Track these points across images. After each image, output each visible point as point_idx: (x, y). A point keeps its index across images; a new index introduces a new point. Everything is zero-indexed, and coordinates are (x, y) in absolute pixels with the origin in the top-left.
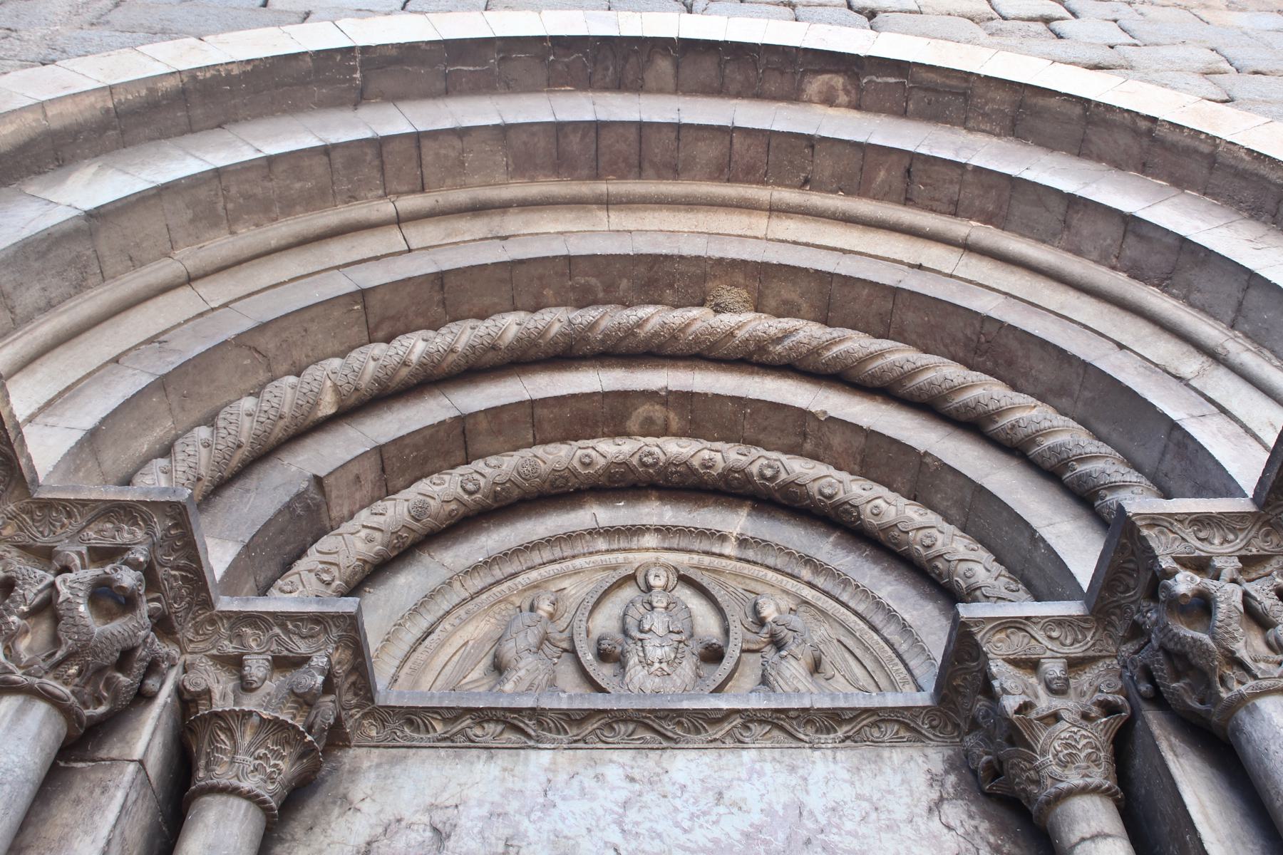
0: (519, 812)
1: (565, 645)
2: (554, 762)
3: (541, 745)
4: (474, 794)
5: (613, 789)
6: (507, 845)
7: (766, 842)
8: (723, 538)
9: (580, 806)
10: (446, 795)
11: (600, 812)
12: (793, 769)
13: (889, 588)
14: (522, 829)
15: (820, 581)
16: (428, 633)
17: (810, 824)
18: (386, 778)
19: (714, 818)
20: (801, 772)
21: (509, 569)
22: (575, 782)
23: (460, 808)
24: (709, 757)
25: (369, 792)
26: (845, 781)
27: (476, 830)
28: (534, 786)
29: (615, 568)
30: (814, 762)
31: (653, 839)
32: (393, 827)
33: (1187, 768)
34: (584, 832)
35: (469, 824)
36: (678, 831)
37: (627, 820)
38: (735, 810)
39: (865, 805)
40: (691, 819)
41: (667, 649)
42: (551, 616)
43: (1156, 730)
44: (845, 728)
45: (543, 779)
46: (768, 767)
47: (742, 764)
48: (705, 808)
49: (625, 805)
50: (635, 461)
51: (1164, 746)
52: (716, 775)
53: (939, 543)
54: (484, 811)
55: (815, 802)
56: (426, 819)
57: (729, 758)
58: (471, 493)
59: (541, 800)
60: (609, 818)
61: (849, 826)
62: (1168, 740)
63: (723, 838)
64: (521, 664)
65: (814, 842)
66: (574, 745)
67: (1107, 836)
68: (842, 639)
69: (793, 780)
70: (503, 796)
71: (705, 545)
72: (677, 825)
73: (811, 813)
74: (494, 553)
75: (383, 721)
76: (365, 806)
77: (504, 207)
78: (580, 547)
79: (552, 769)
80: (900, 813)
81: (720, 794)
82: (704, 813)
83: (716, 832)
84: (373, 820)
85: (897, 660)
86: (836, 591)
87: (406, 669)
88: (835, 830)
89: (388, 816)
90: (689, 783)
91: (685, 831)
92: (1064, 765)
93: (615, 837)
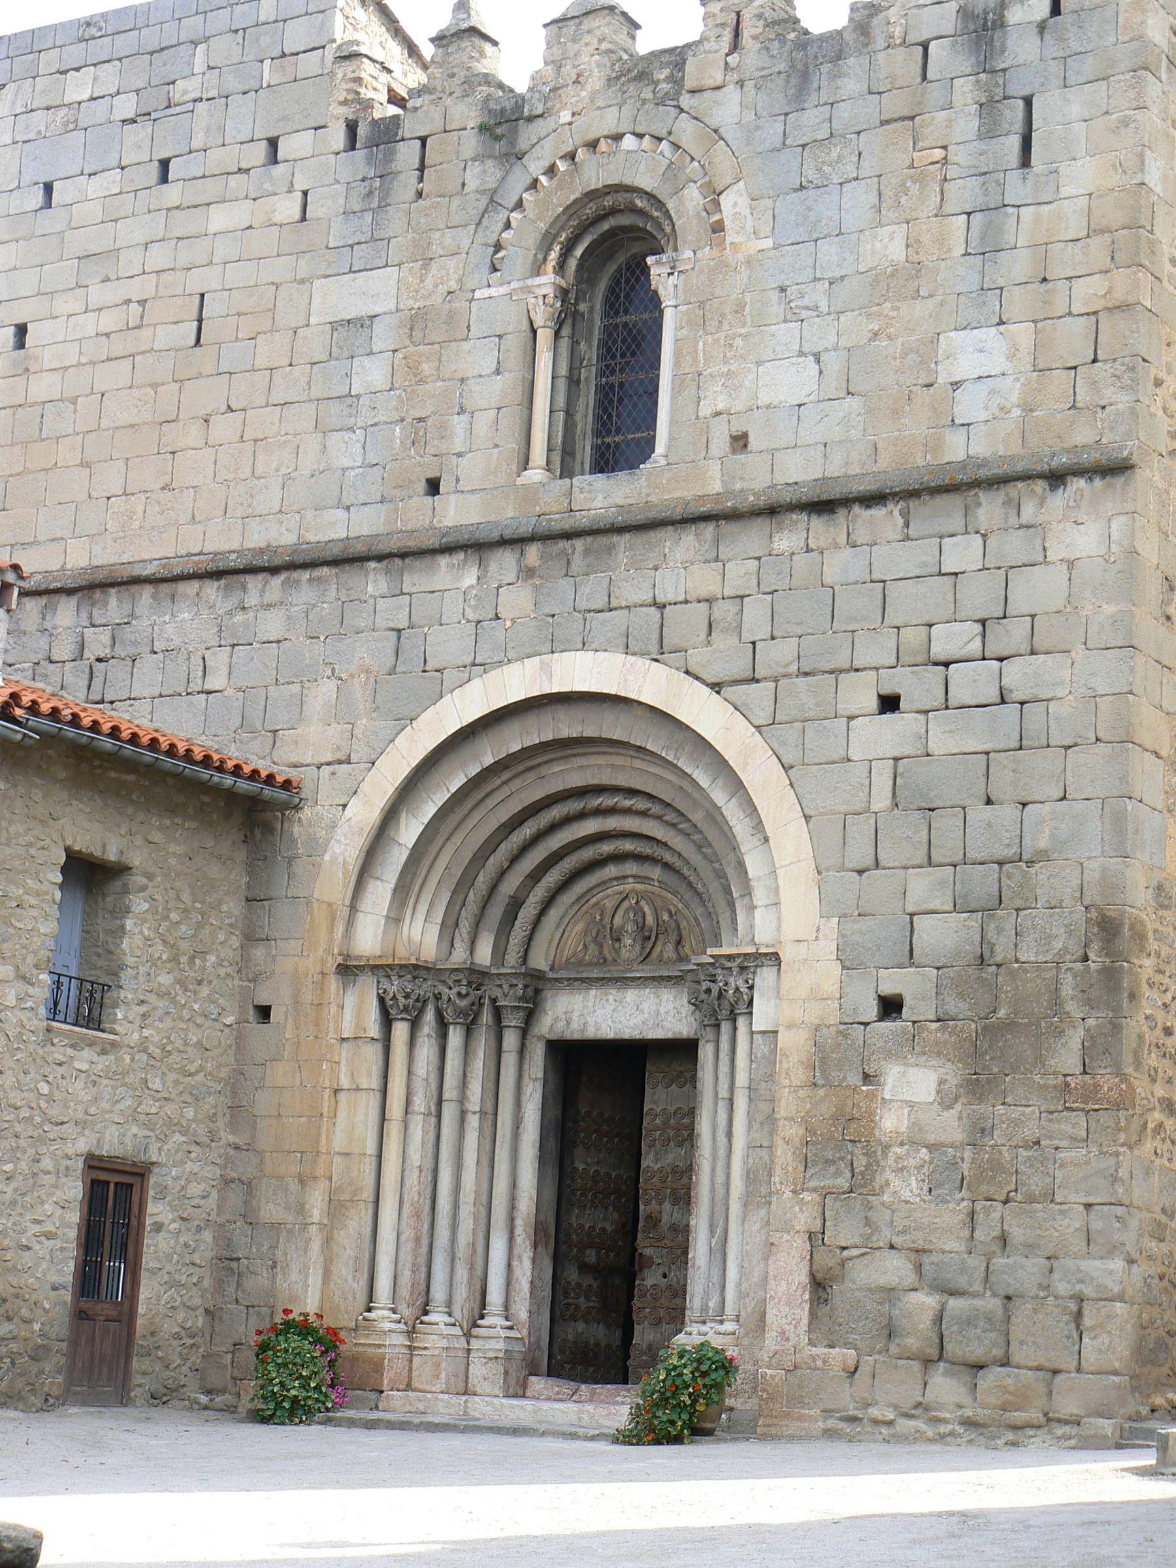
4: (576, 1007)
9: (602, 1011)
28: (590, 1004)
29: (621, 893)
42: (601, 920)
77: (539, 765)
79: (595, 997)
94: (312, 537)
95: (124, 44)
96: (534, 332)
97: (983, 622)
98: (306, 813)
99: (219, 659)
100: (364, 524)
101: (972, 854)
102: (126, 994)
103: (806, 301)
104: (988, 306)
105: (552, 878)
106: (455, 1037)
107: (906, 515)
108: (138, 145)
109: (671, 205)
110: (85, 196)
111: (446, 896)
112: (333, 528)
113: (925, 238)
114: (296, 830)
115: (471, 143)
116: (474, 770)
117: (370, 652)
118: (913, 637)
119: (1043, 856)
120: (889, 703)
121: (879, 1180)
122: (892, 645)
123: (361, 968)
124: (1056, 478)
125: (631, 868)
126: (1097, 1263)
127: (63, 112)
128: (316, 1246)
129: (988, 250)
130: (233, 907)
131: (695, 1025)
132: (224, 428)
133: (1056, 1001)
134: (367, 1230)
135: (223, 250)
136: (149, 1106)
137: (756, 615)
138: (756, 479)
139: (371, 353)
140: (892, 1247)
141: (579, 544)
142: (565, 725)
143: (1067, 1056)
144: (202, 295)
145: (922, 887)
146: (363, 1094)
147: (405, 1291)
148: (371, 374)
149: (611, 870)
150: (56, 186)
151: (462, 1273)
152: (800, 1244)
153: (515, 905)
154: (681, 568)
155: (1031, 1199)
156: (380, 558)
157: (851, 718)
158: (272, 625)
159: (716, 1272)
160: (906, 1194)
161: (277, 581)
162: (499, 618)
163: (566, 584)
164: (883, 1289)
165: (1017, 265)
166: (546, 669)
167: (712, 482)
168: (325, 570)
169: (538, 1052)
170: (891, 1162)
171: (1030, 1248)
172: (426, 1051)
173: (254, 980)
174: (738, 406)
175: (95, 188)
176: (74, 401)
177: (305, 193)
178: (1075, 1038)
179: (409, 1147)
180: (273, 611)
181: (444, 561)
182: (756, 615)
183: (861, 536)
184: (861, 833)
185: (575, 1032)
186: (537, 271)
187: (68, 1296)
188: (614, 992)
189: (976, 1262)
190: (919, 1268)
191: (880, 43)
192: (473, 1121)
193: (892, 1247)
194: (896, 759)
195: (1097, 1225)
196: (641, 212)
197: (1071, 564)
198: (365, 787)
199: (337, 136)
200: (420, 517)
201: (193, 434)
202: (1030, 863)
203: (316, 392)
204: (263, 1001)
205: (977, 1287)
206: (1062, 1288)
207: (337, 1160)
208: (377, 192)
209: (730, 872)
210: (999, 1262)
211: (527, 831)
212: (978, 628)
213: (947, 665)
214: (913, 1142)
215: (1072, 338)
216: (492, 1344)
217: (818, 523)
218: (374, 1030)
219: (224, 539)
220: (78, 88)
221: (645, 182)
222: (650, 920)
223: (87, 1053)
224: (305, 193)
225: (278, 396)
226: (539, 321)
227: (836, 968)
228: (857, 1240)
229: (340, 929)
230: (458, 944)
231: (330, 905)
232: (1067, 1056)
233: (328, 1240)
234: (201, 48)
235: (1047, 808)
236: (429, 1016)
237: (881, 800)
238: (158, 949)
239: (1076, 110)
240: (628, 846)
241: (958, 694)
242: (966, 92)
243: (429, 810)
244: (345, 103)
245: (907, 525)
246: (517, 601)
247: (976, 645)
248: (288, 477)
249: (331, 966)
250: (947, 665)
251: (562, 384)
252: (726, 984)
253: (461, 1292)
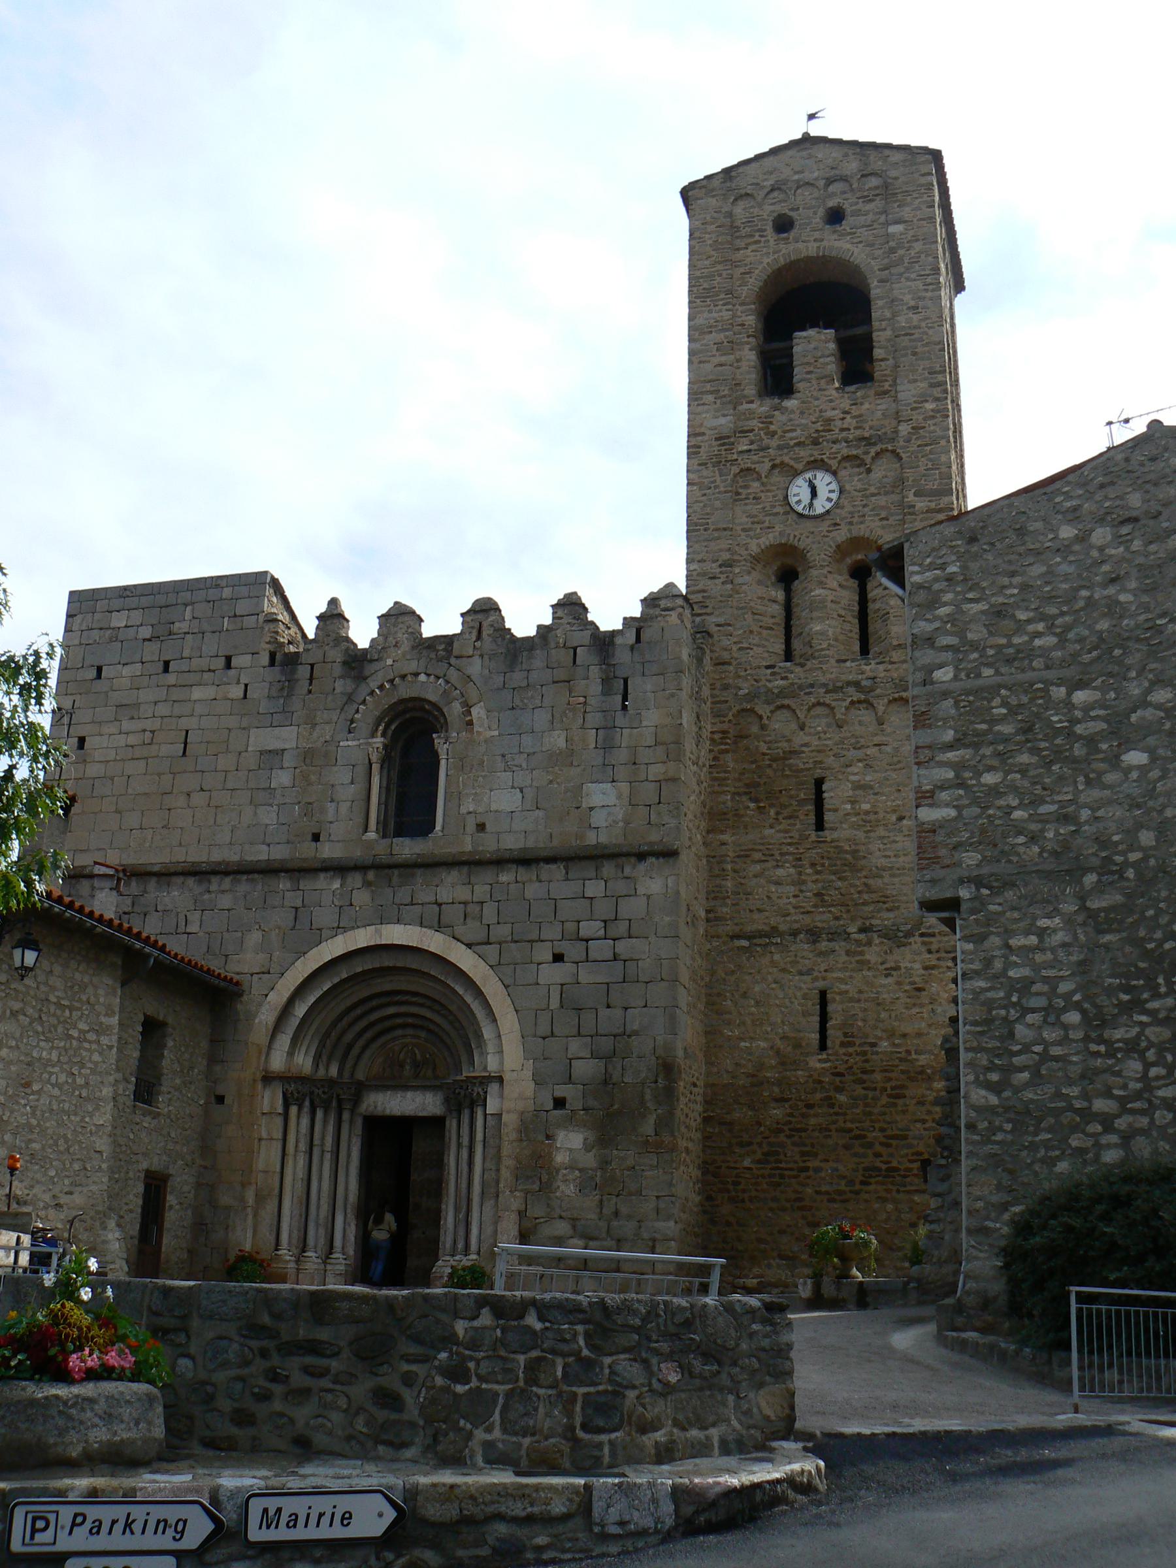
94: (248, 858)
95: (145, 601)
96: (371, 765)
97: (605, 922)
98: (245, 998)
99: (195, 917)
100: (279, 853)
101: (601, 1031)
102: (164, 1089)
103: (515, 762)
104: (607, 772)
106: (320, 1114)
107: (566, 868)
108: (152, 651)
109: (445, 710)
110: (122, 675)
112: (261, 854)
113: (576, 738)
114: (239, 1007)
115: (338, 669)
116: (336, 980)
117: (280, 918)
118: (570, 927)
119: (636, 1033)
120: (558, 958)
121: (555, 1185)
122: (559, 929)
123: (274, 1078)
124: (641, 856)
125: (410, 1031)
126: (663, 1224)
127: (109, 632)
128: (250, 1217)
129: (607, 747)
130: (204, 1044)
132: (198, 799)
133: (643, 1103)
134: (276, 1210)
135: (199, 709)
136: (170, 1146)
137: (489, 911)
138: (489, 845)
139: (282, 768)
140: (561, 1217)
141: (396, 872)
142: (387, 961)
143: (648, 1127)
144: (187, 732)
145: (576, 1047)
146: (274, 1142)
147: (294, 1241)
148: (282, 778)
149: (399, 1032)
150: (104, 668)
151: (322, 1231)
152: (514, 1217)
153: (350, 1047)
154: (450, 888)
155: (630, 1194)
156: (287, 871)
157: (539, 964)
158: (225, 901)
159: (461, 1232)
160: (568, 1192)
161: (228, 880)
162: (351, 905)
163: (389, 892)
164: (555, 1237)
165: (622, 755)
166: (378, 932)
167: (467, 845)
168: (256, 876)
169: (359, 1122)
170: (560, 1177)
171: (629, 1217)
172: (305, 1121)
173: (215, 1082)
174: (480, 810)
175: (126, 671)
176: (112, 779)
177: (246, 685)
178: (652, 1119)
179: (296, 1168)
180: (226, 895)
181: (322, 875)
182: (489, 911)
183: (544, 877)
184: (544, 1019)
185: (379, 1111)
186: (373, 736)
187: (136, 1242)
189: (603, 1224)
190: (574, 1227)
191: (553, 645)
192: (328, 1156)
193: (561, 1217)
194: (562, 985)
195: (662, 1205)
196: (428, 712)
197: (648, 897)
198: (278, 986)
199: (265, 660)
200: (307, 850)
201: (182, 801)
202: (629, 1036)
203: (252, 785)
204: (220, 1092)
205: (604, 1235)
206: (646, 1235)
207: (260, 1176)
208: (287, 687)
209: (471, 1035)
210: (615, 1223)
211: (359, 1011)
212: (603, 924)
213: (587, 941)
214: (571, 1167)
215: (648, 792)
216: (338, 1267)
217: (522, 870)
218: (280, 1110)
219: (197, 855)
220: (119, 620)
221: (432, 698)
222: (419, 1057)
223: (148, 1119)
224: (246, 685)
225: (230, 785)
226: (374, 758)
227: (532, 1085)
228: (543, 1214)
229: (263, 1058)
230: (321, 1066)
231: (258, 1045)
232: (648, 1127)
233: (255, 1215)
234: (189, 608)
235: (636, 1011)
236: (307, 1103)
237: (555, 1003)
238: (176, 1067)
239: (649, 687)
241: (593, 955)
242: (595, 672)
243: (312, 999)
244: (269, 643)
245: (567, 873)
246: (362, 897)
247: (602, 932)
248: (234, 827)
249: (259, 1076)
250: (587, 941)
251: (384, 790)
253: (322, 1241)
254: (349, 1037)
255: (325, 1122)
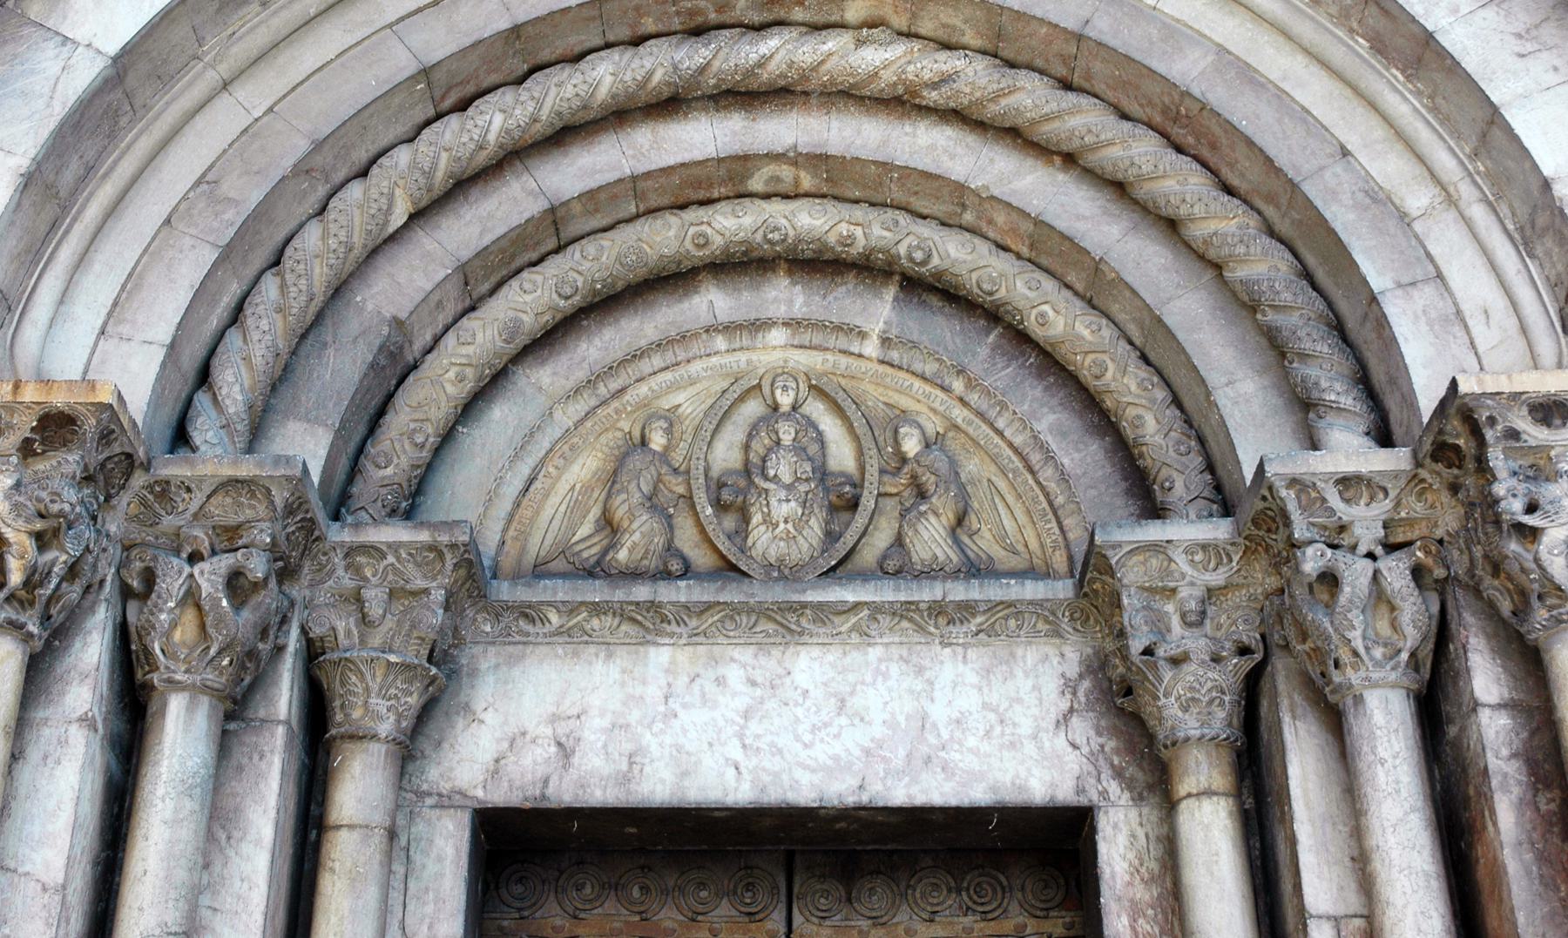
0: (640, 722)
1: (681, 490)
2: (673, 662)
3: (659, 640)
4: (595, 701)
5: (734, 694)
6: (631, 764)
7: (885, 759)
8: (863, 335)
9: (700, 716)
10: (567, 703)
11: (721, 723)
12: (920, 671)
13: (1052, 418)
14: (644, 743)
15: (974, 398)
16: (531, 481)
17: (932, 740)
18: (506, 682)
19: (834, 730)
20: (928, 674)
21: (614, 385)
22: (696, 687)
23: (583, 718)
24: (833, 655)
25: (491, 700)
26: (973, 686)
27: (600, 744)
28: (654, 692)
30: (942, 662)
31: (773, 755)
32: (519, 742)
33: (1302, 733)
34: (706, 746)
35: (592, 737)
36: (799, 746)
37: (748, 733)
38: (857, 721)
39: (992, 717)
40: (812, 732)
41: (793, 504)
43: (1282, 685)
44: (979, 619)
45: (663, 682)
46: (894, 669)
47: (867, 664)
48: (826, 719)
49: (747, 715)
50: (759, 237)
51: (1284, 704)
52: (839, 678)
53: (1109, 375)
54: (605, 722)
55: (939, 712)
56: (549, 731)
57: (855, 657)
58: (567, 298)
59: (662, 708)
60: (730, 730)
61: (972, 742)
62: (1291, 697)
63: (843, 755)
64: (635, 526)
65: (935, 760)
66: (695, 639)
67: (1215, 794)
68: (994, 478)
69: (919, 685)
70: (624, 704)
71: (842, 342)
72: (797, 738)
73: (934, 725)
74: (597, 368)
75: (497, 615)
76: (489, 717)
78: (696, 348)
80: (1026, 727)
81: (843, 701)
82: (826, 725)
83: (837, 748)
84: (498, 734)
85: (1051, 516)
86: (992, 414)
87: (511, 533)
88: (956, 747)
89: (512, 729)
90: (811, 688)
91: (806, 746)
92: (1185, 709)
93: (736, 753)
105: (530, 299)
106: (181, 737)
111: (190, 265)
131: (1074, 763)
149: (713, 301)
169: (446, 852)
185: (593, 780)
188: (745, 654)
222: (842, 455)
236: (92, 650)
240: (811, 221)
252: (1531, 508)
254: (408, 282)
255: (217, 817)
